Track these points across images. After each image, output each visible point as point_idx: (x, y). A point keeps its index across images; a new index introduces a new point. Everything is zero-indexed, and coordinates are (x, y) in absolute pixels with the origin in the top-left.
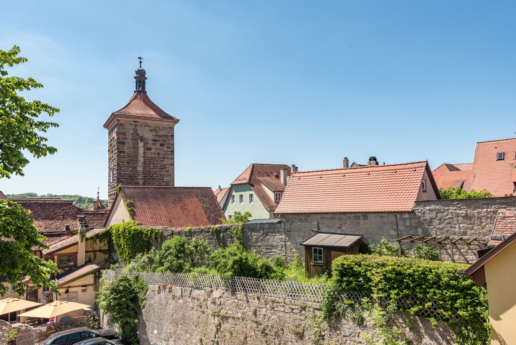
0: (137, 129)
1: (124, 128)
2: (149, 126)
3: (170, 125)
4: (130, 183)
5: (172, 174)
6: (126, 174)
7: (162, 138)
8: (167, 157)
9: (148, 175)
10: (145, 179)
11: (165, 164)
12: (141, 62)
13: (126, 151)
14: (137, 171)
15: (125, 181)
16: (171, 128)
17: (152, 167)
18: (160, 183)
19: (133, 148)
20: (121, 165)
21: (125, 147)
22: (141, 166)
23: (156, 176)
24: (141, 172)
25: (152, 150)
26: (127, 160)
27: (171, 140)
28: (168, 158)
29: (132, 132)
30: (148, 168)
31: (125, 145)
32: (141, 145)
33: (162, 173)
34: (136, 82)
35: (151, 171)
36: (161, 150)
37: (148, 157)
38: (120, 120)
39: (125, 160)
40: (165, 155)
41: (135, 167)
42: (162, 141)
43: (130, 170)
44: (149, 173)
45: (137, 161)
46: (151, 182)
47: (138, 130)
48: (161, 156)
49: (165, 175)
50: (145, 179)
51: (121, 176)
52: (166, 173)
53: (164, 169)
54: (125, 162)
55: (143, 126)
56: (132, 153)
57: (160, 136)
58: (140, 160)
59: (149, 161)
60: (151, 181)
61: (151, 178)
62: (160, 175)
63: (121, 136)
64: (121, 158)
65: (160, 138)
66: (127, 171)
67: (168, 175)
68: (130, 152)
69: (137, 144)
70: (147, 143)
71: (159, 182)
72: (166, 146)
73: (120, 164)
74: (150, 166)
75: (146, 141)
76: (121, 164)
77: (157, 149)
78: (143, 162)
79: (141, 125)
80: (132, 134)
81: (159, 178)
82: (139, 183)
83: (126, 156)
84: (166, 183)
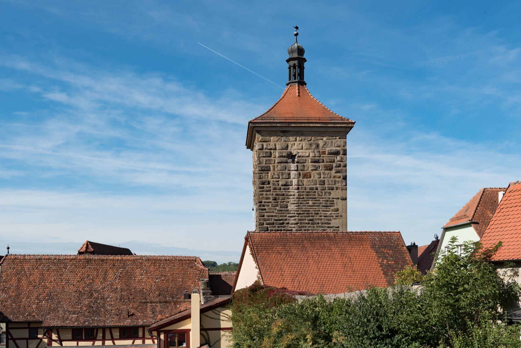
5: (344, 214)
7: (326, 155)
10: (301, 223)
11: (333, 198)
15: (270, 227)
20: (265, 202)
21: (269, 174)
22: (294, 204)
24: (293, 212)
25: (312, 176)
30: (305, 206)
33: (329, 213)
34: (290, 68)
35: (309, 211)
46: (310, 228)
53: (331, 206)
58: (292, 193)
60: (310, 227)
61: (310, 222)
64: (263, 191)
66: (274, 212)
68: (277, 181)
74: (309, 203)
76: (263, 201)
78: (296, 196)
81: (323, 221)
83: (272, 189)
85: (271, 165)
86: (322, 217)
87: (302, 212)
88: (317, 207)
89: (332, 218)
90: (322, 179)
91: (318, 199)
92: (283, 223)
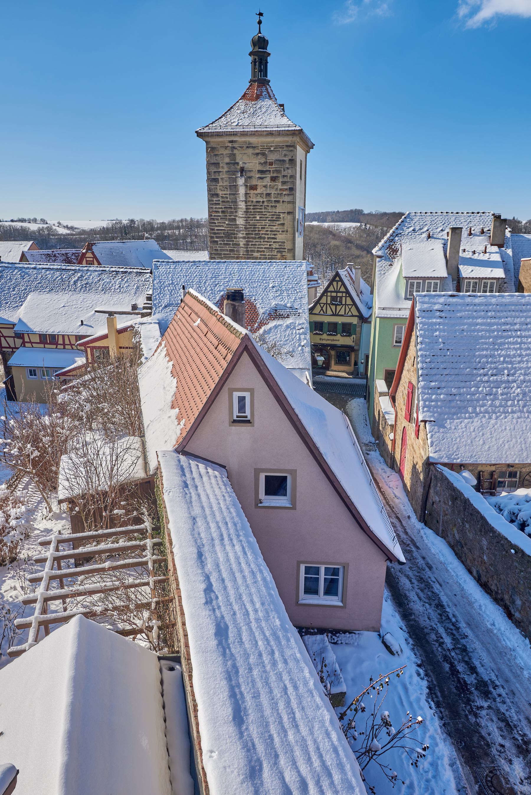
0: (234, 155)
1: (216, 155)
2: (253, 147)
3: (288, 141)
4: (227, 244)
5: (289, 230)
6: (221, 230)
7: (273, 166)
8: (281, 200)
9: (252, 231)
10: (248, 238)
11: (279, 212)
12: (260, 22)
13: (220, 193)
14: (237, 226)
16: (290, 146)
17: (258, 218)
18: (270, 245)
19: (230, 189)
21: (218, 187)
23: (264, 232)
26: (221, 208)
27: (288, 168)
28: (283, 202)
29: (227, 160)
31: (219, 183)
32: (241, 181)
33: (274, 227)
36: (273, 188)
37: (252, 202)
38: (210, 142)
39: (219, 208)
40: (279, 196)
41: (233, 219)
42: (273, 173)
43: (227, 224)
44: (254, 228)
45: (236, 209)
46: (257, 243)
47: (237, 155)
48: (273, 199)
49: (279, 231)
50: (248, 238)
51: (215, 233)
52: (279, 228)
54: (218, 212)
55: (245, 148)
56: (228, 196)
57: (271, 164)
58: (240, 206)
59: (253, 209)
62: (270, 231)
63: (213, 169)
64: (213, 204)
65: (270, 167)
66: (223, 226)
67: (283, 231)
69: (235, 180)
70: (250, 177)
71: (269, 244)
72: (281, 180)
73: (212, 215)
75: (249, 174)
76: (213, 215)
77: (265, 186)
79: (240, 147)
80: (227, 164)
81: (269, 236)
82: (239, 245)
84: (280, 244)
85: (219, 177)
86: (269, 233)
87: (249, 227)
88: (264, 222)
89: (278, 233)
90: (268, 192)
91: (265, 213)
92: (232, 238)
